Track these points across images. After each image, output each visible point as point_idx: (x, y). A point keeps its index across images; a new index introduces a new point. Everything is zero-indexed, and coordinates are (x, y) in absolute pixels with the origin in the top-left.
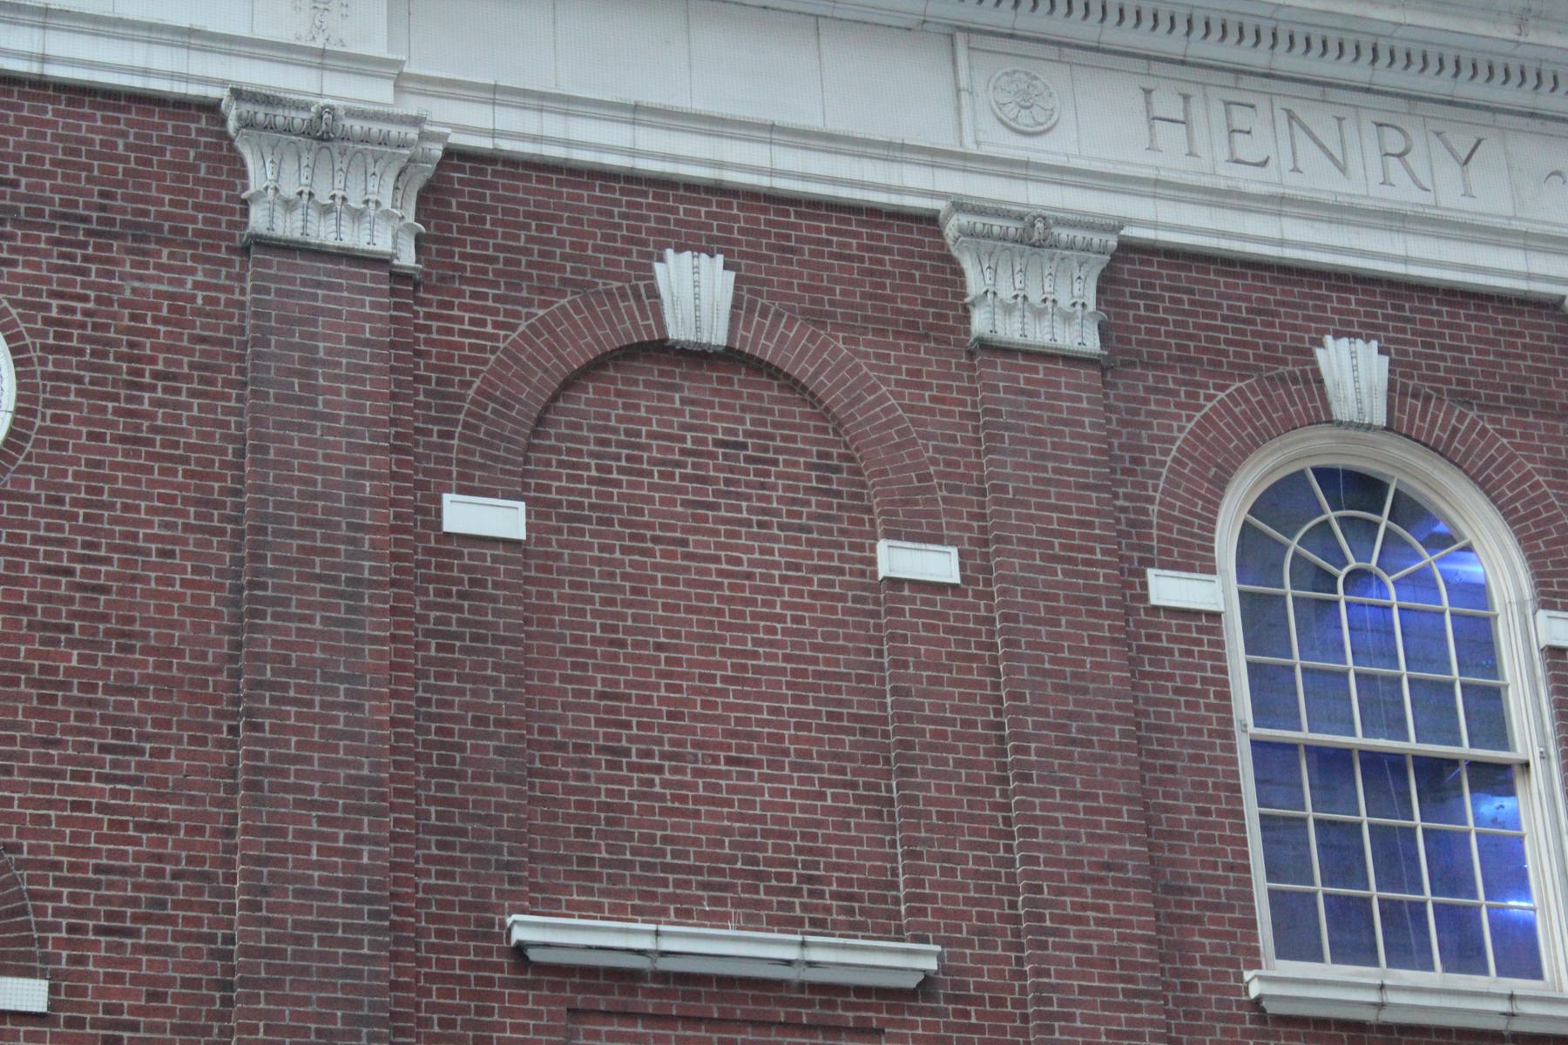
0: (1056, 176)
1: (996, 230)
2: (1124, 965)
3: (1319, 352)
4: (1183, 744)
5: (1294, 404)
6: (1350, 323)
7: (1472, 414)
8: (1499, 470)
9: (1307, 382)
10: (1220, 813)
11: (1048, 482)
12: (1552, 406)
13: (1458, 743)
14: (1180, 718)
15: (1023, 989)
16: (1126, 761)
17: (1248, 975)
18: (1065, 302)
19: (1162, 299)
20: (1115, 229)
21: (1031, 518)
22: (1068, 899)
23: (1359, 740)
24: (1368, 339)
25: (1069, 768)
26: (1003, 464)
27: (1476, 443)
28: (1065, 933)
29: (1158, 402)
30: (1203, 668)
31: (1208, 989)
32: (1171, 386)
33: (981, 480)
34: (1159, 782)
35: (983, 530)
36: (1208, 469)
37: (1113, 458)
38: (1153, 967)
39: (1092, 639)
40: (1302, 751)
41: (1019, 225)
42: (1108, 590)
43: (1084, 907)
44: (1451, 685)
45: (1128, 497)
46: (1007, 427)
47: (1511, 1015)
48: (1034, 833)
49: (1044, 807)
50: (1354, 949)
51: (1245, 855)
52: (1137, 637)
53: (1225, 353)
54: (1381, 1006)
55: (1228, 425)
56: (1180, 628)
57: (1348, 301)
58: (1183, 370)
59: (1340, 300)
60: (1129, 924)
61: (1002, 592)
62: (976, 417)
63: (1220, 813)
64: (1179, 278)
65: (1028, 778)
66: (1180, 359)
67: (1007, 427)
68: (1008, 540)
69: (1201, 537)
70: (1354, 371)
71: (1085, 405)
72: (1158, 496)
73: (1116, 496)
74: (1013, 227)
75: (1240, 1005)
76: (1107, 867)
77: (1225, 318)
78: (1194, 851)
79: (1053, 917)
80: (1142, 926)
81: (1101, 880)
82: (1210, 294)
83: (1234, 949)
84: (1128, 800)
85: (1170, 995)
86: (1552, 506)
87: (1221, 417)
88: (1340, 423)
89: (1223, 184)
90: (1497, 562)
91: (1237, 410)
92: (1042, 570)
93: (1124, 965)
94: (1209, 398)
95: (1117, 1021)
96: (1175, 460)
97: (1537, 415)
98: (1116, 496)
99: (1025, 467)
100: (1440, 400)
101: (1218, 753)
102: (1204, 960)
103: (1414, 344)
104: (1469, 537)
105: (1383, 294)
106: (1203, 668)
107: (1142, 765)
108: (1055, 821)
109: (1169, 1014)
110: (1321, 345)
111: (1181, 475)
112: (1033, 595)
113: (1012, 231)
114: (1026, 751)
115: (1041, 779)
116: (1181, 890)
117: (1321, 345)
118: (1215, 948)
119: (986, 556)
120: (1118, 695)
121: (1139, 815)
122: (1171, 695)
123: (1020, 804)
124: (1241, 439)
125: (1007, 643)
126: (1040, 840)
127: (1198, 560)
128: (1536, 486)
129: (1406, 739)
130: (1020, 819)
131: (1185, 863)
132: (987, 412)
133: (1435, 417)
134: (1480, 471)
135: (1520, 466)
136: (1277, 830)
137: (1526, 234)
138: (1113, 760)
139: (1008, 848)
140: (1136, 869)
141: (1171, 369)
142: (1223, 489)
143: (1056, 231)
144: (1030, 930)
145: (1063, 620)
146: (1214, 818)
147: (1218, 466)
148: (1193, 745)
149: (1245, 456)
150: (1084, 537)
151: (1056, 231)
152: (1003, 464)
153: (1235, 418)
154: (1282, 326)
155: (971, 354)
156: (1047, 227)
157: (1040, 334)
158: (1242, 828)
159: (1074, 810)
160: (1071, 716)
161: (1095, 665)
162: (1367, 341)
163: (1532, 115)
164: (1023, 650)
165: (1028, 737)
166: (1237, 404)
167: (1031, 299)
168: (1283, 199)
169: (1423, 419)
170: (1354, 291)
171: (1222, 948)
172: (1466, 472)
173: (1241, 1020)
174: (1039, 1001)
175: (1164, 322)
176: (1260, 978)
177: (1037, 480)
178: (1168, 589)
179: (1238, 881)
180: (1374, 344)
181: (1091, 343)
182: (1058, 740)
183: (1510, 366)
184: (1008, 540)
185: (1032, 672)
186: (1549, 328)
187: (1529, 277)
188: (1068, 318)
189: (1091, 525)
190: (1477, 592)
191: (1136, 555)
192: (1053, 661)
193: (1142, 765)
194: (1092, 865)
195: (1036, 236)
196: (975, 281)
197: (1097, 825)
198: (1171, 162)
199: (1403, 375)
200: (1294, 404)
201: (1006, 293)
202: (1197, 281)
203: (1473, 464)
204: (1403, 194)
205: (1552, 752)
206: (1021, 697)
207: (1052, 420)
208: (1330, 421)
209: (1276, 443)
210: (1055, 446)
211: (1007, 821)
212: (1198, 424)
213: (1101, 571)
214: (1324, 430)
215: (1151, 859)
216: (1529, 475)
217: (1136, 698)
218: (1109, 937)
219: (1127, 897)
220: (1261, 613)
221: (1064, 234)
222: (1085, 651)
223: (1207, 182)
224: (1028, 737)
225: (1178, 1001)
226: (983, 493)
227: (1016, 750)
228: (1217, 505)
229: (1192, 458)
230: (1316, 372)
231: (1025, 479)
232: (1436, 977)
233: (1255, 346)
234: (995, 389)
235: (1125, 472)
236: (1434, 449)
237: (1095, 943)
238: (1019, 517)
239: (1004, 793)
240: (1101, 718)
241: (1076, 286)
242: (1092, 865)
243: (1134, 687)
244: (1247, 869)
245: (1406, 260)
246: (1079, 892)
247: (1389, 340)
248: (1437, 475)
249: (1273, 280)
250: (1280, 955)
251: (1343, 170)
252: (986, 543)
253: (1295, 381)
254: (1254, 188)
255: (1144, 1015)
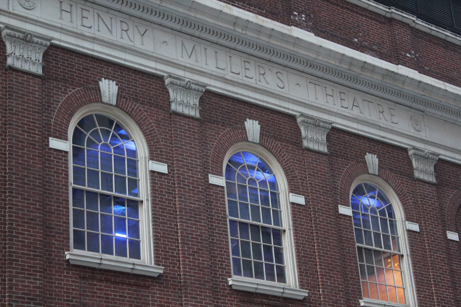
0: (35, 23)
1: (17, 35)
2: (34, 247)
3: (100, 82)
4: (55, 187)
5: (92, 96)
6: (109, 76)
7: (138, 105)
8: (143, 121)
9: (96, 90)
10: (63, 207)
11: (24, 109)
12: (158, 105)
13: (112, 191)
14: (55, 180)
15: (5, 251)
16: (39, 190)
17: (66, 253)
18: (33, 59)
19: (60, 62)
20: (49, 40)
21: (20, 119)
22: (20, 228)
23: (100, 190)
24: (113, 81)
25: (24, 191)
26: (13, 103)
27: (138, 113)
28: (18, 237)
29: (56, 91)
30: (62, 167)
31: (55, 256)
32: (60, 86)
33: (6, 106)
34: (47, 197)
35: (5, 121)
36: (68, 111)
37: (43, 105)
38: (41, 249)
39: (33, 155)
40: (85, 192)
41: (23, 35)
42: (39, 142)
43: (24, 230)
44: (112, 175)
45: (46, 116)
46: (15, 92)
47: (133, 269)
48: (12, 208)
49: (16, 201)
50: (93, 248)
51: (68, 220)
52: (45, 156)
53: (75, 79)
54: (100, 264)
55: (74, 99)
56: (57, 155)
57: (109, 69)
58: (64, 83)
59: (107, 69)
60: (36, 236)
61: (10, 139)
62: (6, 88)
63: (63, 207)
64: (65, 56)
65: (12, 193)
66: (63, 79)
67: (15, 92)
68: (12, 125)
69: (65, 130)
70: (109, 89)
71: (37, 89)
72: (54, 117)
73: (43, 116)
74: (21, 35)
75: (63, 261)
76: (32, 220)
77: (76, 69)
78: (55, 217)
79: (16, 233)
80: (40, 237)
81: (30, 223)
82: (73, 62)
83: (63, 245)
84: (39, 202)
85: (45, 257)
86: (155, 133)
87: (73, 97)
88: (104, 103)
89: (79, 32)
90: (138, 144)
91: (77, 96)
92: (21, 134)
93: (34, 247)
94: (70, 91)
95: (30, 263)
96: (59, 107)
97: (154, 107)
98: (43, 116)
99: (18, 104)
100: (130, 100)
101: (64, 191)
102: (55, 248)
103: (125, 83)
104: (134, 138)
105: (118, 69)
106: (62, 167)
107: (43, 192)
108: (18, 206)
109: (44, 261)
110: (101, 81)
111: (61, 112)
112: (18, 141)
113: (21, 37)
114: (12, 185)
115: (16, 193)
116: (51, 228)
117: (101, 81)
118: (58, 245)
119: (6, 129)
120: (38, 172)
121: (42, 206)
122: (53, 173)
123: (9, 200)
124: (77, 104)
125: (9, 154)
126: (14, 210)
127: (63, 136)
128: (152, 127)
129: (112, 191)
130: (8, 204)
131: (53, 221)
132: (9, 87)
133: (128, 105)
134: (139, 120)
135: (148, 121)
136: (78, 214)
137: (156, 58)
138: (36, 190)
139: (5, 212)
140: (39, 221)
141: (61, 82)
142: (71, 117)
143: (33, 38)
144: (9, 236)
145: (26, 149)
146: (61, 209)
147: (71, 110)
148: (57, 188)
149: (78, 109)
150: (33, 126)
151: (33, 38)
152: (13, 103)
153: (76, 98)
154: (91, 74)
155: (6, 70)
156: (31, 37)
157: (26, 67)
158: (68, 212)
159: (24, 203)
160: (26, 176)
161: (33, 163)
162: (113, 81)
163: (160, 25)
164: (14, 156)
165: (13, 181)
166: (77, 94)
167: (16, 54)
168: (94, 38)
169: (125, 105)
170: (111, 67)
171: (60, 245)
172: (135, 120)
173: (63, 265)
174: (10, 256)
175: (60, 68)
176: (70, 254)
177: (22, 109)
178: (55, 143)
179: (66, 227)
180: (115, 82)
181: (40, 72)
182: (22, 183)
183: (149, 93)
184: (12, 125)
185: (16, 163)
186: (159, 84)
187: (156, 69)
188: (34, 63)
189: (35, 123)
190: (133, 153)
191: (47, 133)
192: (22, 160)
193: (43, 192)
194: (28, 219)
195: (28, 39)
196: (9, 49)
197: (30, 208)
198: (65, 23)
199: (121, 92)
200: (92, 96)
201: (17, 54)
202: (69, 58)
203: (137, 118)
204: (125, 42)
205: (149, 199)
206: (12, 170)
207: (27, 92)
208: (101, 102)
209: (86, 106)
210: (28, 99)
211: (5, 204)
212: (66, 98)
213: (37, 136)
214: (99, 104)
215: (43, 218)
216: (150, 123)
217: (43, 173)
218: (30, 239)
219: (36, 228)
220: (77, 152)
221: (35, 39)
222: (30, 158)
223: (75, 30)
224: (13, 181)
225: (47, 258)
226: (6, 110)
227: (9, 184)
228: (70, 122)
229: (64, 107)
230: (99, 88)
231: (19, 108)
232: (114, 257)
233: (83, 78)
234: (12, 81)
235: (46, 109)
236: (127, 113)
237: (26, 241)
238: (16, 118)
239: (5, 196)
240: (33, 178)
241: (37, 55)
242: (28, 219)
243: (43, 170)
244: (68, 223)
245: (125, 60)
246: (24, 226)
247: (118, 81)
248: (127, 120)
249: (90, 60)
250: (75, 248)
251: (111, 32)
252: (6, 125)
253: (93, 90)
254: (87, 34)
255: (38, 262)
